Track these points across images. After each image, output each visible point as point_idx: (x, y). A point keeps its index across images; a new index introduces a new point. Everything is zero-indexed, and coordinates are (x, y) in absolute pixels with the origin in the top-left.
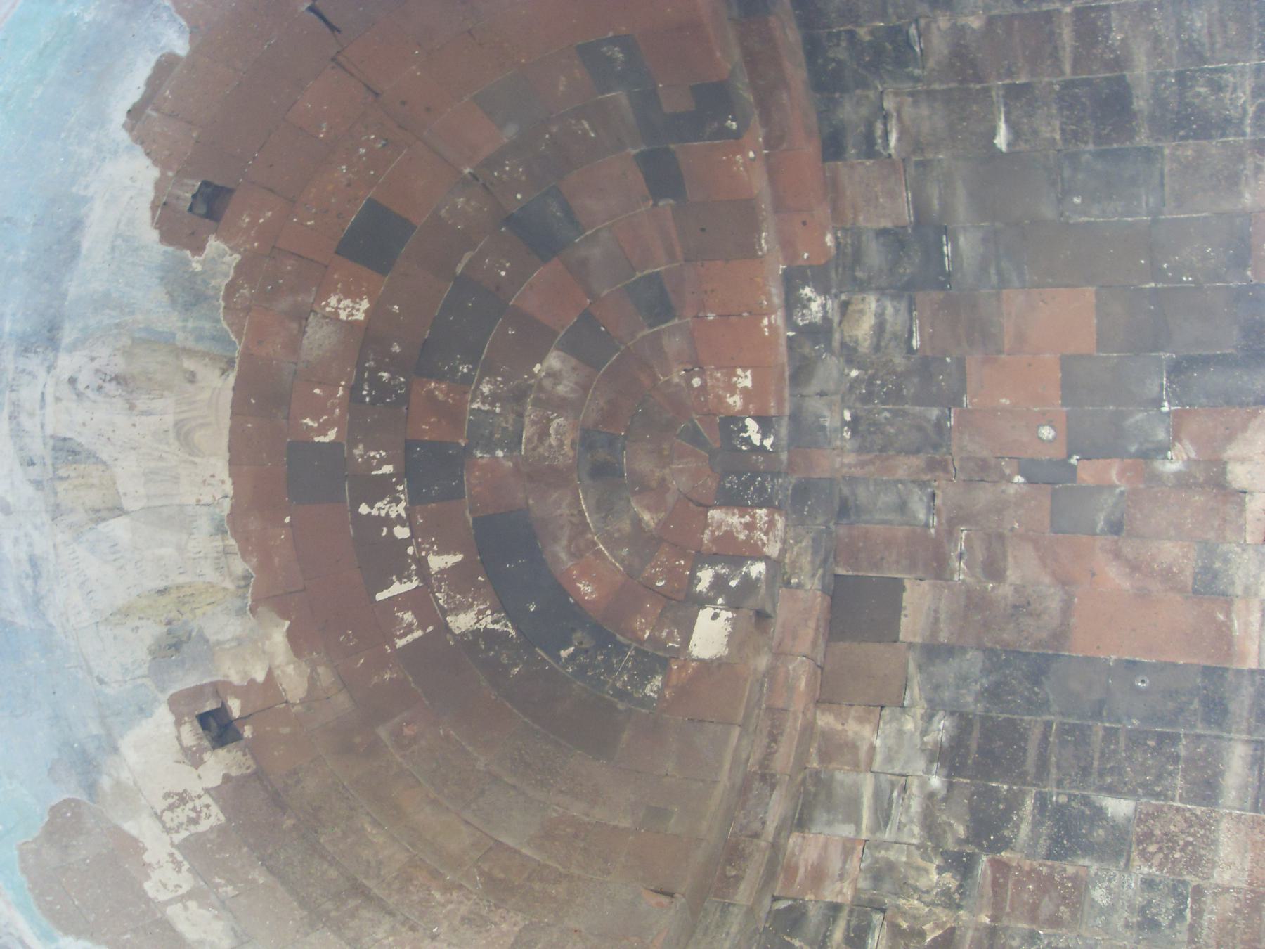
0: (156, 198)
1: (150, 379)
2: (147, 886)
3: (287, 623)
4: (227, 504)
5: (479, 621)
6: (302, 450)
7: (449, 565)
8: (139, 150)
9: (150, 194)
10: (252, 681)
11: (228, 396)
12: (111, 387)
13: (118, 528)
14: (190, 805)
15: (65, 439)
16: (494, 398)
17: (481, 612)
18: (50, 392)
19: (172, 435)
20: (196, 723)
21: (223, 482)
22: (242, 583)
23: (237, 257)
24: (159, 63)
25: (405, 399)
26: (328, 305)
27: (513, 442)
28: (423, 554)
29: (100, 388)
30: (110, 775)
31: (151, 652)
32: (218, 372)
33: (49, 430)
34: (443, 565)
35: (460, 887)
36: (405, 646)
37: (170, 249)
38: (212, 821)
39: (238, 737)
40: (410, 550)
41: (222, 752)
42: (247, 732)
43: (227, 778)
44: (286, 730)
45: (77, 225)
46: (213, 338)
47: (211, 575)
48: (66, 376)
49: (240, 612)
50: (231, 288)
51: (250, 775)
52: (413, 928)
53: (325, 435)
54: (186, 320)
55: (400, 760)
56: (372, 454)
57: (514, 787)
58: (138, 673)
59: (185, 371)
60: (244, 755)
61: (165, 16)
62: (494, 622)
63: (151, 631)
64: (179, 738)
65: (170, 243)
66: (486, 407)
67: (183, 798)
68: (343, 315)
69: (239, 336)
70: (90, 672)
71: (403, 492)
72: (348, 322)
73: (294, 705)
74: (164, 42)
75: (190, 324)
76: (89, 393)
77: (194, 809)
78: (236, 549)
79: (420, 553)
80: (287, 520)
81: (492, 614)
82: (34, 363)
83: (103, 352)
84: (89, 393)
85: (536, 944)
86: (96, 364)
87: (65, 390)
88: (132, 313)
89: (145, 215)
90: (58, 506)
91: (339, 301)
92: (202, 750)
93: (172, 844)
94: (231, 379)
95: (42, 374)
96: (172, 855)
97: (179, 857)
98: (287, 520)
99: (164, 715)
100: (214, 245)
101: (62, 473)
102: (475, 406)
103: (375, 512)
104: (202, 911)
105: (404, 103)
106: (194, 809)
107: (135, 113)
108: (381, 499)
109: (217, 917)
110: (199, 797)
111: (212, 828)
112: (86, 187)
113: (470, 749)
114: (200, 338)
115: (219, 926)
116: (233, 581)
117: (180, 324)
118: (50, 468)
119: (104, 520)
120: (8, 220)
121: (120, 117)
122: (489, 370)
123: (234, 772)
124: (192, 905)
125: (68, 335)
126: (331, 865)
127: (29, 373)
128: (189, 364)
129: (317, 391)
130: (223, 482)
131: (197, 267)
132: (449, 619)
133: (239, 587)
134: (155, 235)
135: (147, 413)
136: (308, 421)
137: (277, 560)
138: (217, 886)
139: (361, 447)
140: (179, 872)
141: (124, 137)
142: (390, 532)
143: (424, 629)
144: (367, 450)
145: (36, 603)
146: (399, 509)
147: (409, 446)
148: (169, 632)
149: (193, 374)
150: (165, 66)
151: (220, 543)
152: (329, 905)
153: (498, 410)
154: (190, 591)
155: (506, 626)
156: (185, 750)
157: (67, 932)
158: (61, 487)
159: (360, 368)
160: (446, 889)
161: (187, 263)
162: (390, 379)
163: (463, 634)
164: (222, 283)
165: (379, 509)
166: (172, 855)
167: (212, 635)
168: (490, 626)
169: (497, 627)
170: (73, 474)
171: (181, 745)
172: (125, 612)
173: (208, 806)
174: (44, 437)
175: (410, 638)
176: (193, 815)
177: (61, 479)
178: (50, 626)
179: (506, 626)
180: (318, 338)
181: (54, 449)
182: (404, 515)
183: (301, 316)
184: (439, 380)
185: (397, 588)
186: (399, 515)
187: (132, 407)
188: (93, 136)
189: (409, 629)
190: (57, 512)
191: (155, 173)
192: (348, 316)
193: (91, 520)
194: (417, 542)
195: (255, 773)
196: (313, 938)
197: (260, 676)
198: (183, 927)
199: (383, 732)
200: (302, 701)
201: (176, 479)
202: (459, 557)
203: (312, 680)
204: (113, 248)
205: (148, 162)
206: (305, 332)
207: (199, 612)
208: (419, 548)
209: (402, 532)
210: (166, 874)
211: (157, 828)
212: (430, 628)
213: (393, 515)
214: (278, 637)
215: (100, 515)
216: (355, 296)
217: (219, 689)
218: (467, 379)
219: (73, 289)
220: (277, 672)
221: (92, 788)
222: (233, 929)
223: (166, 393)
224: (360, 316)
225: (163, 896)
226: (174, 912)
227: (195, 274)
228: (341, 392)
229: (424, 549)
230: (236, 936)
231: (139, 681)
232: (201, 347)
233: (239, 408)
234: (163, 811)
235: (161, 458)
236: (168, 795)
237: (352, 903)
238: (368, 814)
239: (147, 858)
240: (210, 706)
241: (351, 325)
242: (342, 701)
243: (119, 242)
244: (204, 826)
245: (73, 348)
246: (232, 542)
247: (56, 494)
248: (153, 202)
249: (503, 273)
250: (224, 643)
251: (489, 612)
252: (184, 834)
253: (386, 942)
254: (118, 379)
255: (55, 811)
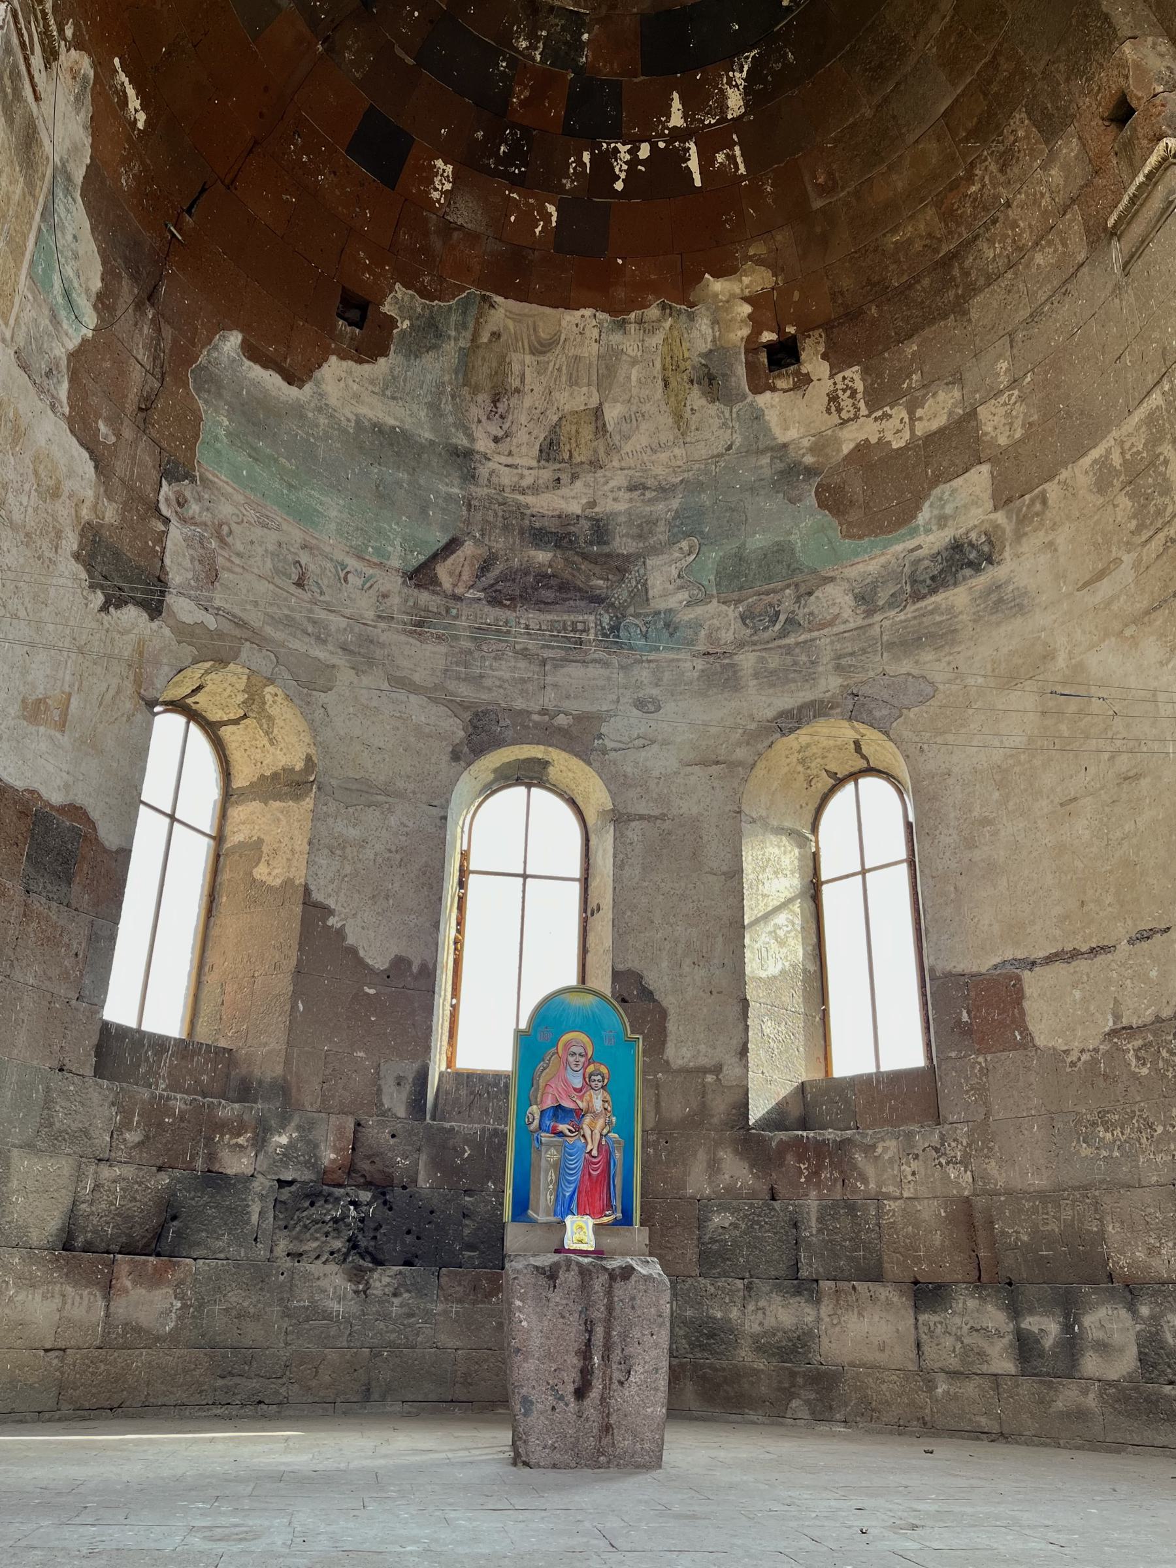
0: (352, 360)
1: (496, 373)
2: (895, 446)
3: (707, 276)
4: (600, 315)
5: (737, 86)
6: (561, 237)
7: (680, 107)
8: (317, 374)
9: (351, 363)
10: (750, 316)
11: (511, 302)
12: (501, 408)
13: (612, 414)
14: (840, 393)
15: (541, 451)
16: (532, 37)
17: (729, 82)
18: (504, 460)
19: (541, 358)
20: (776, 373)
21: (583, 316)
22: (668, 311)
23: (398, 286)
24: (249, 358)
25: (526, 130)
26: (438, 201)
27: (576, 21)
28: (667, 132)
29: (501, 417)
30: (803, 455)
31: (713, 401)
32: (492, 311)
33: (534, 463)
34: (680, 114)
35: (972, 165)
36: (746, 166)
37: (392, 348)
38: (857, 377)
39: (794, 338)
40: (662, 145)
41: (803, 356)
42: (791, 330)
43: (825, 357)
44: (796, 295)
45: (378, 429)
46: (464, 313)
47: (657, 339)
48: (493, 445)
49: (691, 317)
50: (423, 293)
51: (827, 336)
52: (995, 222)
53: (551, 215)
54: (449, 337)
55: (845, 193)
56: (572, 171)
57: (898, 84)
58: (727, 415)
59: (490, 341)
60: (809, 336)
61: (215, 354)
62: (741, 71)
63: (696, 398)
64: (785, 391)
65: (388, 348)
66: (541, 45)
67: (833, 398)
68: (448, 186)
69: (463, 289)
70: (722, 455)
71: (608, 144)
72: (454, 183)
73: (776, 283)
74: (233, 354)
75: (453, 333)
76: (506, 426)
77: (844, 391)
78: (640, 312)
79: (666, 135)
80: (620, 261)
81: (734, 71)
82: (483, 471)
83: (475, 412)
84: (506, 426)
85: (1046, 108)
86: (484, 419)
87: (504, 447)
88: (443, 383)
89: (366, 366)
90: (591, 463)
91: (436, 190)
92: (798, 373)
93: (867, 416)
94: (499, 299)
95: (490, 465)
96: (876, 419)
97: (880, 413)
98: (620, 261)
99: (764, 400)
100: (388, 308)
101: (566, 456)
102: (538, 58)
103: (623, 175)
104: (926, 406)
105: (261, 115)
106: (844, 391)
107: (290, 379)
108: (613, 168)
109: (934, 395)
110: (835, 384)
111: (863, 379)
112: (349, 420)
113: (851, 120)
114: (464, 326)
115: (941, 395)
116: (666, 320)
117: (452, 342)
118: (563, 465)
119: (604, 425)
120: (377, 487)
121: (293, 392)
122: (506, 39)
123: (822, 349)
124: (919, 412)
125: (461, 441)
126: (918, 282)
127: (490, 475)
128: (485, 338)
129: (512, 219)
130: (583, 316)
131: (406, 323)
132: (730, 117)
133: (671, 315)
134: (382, 361)
135: (523, 376)
136: (537, 231)
137: (653, 277)
138: (910, 387)
139: (564, 181)
140: (891, 416)
141: (308, 387)
142: (642, 162)
143: (735, 144)
144: (568, 176)
145: (664, 491)
146: (623, 149)
147: (568, 132)
148: (699, 383)
149: (493, 334)
150: (252, 352)
151: (633, 326)
152: (952, 293)
153: (544, 33)
154: (668, 359)
155: (747, 57)
156: (795, 388)
157: (914, 517)
158: (577, 459)
159: (495, 173)
160: (970, 178)
161: (403, 332)
162: (506, 144)
163: (746, 105)
164: (419, 301)
165: (621, 170)
166: (876, 419)
167: (704, 346)
168: (744, 74)
169: (746, 68)
170: (567, 447)
171: (791, 390)
172: (678, 417)
173: (844, 378)
174: (539, 468)
175: (739, 160)
176: (848, 392)
177: (571, 457)
178: (682, 481)
179: (747, 57)
180: (466, 215)
181: (548, 461)
182: (629, 147)
183: (448, 228)
184: (509, 93)
185: (693, 164)
186: (629, 151)
187: (517, 391)
188: (310, 415)
189: (732, 158)
190: (596, 464)
191: (333, 359)
192: (449, 181)
193: (604, 435)
194: (654, 137)
195: (826, 331)
196: (974, 314)
197: (747, 309)
198: (935, 425)
199: (817, 204)
200: (775, 275)
201: (577, 358)
202: (675, 95)
203: (760, 262)
204: (394, 398)
205: (325, 365)
206: (462, 226)
207: (686, 355)
208: (661, 136)
209: (644, 151)
210: (890, 425)
211: (852, 426)
212: (735, 137)
213: (628, 157)
214: (718, 286)
215: (601, 429)
216: (432, 172)
217: (752, 347)
218: (513, 63)
219: (427, 435)
220: (747, 292)
221: (810, 472)
222: (947, 384)
223: (508, 360)
224: (449, 169)
225: (907, 435)
226: (921, 429)
227: (412, 326)
228: (515, 195)
229: (663, 131)
230: (954, 383)
231: (734, 416)
232: (471, 325)
233: (522, 295)
234: (840, 418)
235: (559, 370)
236: (828, 411)
237: (956, 272)
238: (884, 235)
239: (874, 440)
240: (764, 358)
241: (457, 178)
242: (781, 237)
243: (388, 393)
244: (859, 386)
245: (472, 438)
246: (633, 315)
247: (582, 463)
248: (356, 362)
249: (416, 14)
250: (714, 337)
251: (731, 74)
252: (862, 405)
253: (998, 250)
254: (495, 401)
255: (822, 504)
